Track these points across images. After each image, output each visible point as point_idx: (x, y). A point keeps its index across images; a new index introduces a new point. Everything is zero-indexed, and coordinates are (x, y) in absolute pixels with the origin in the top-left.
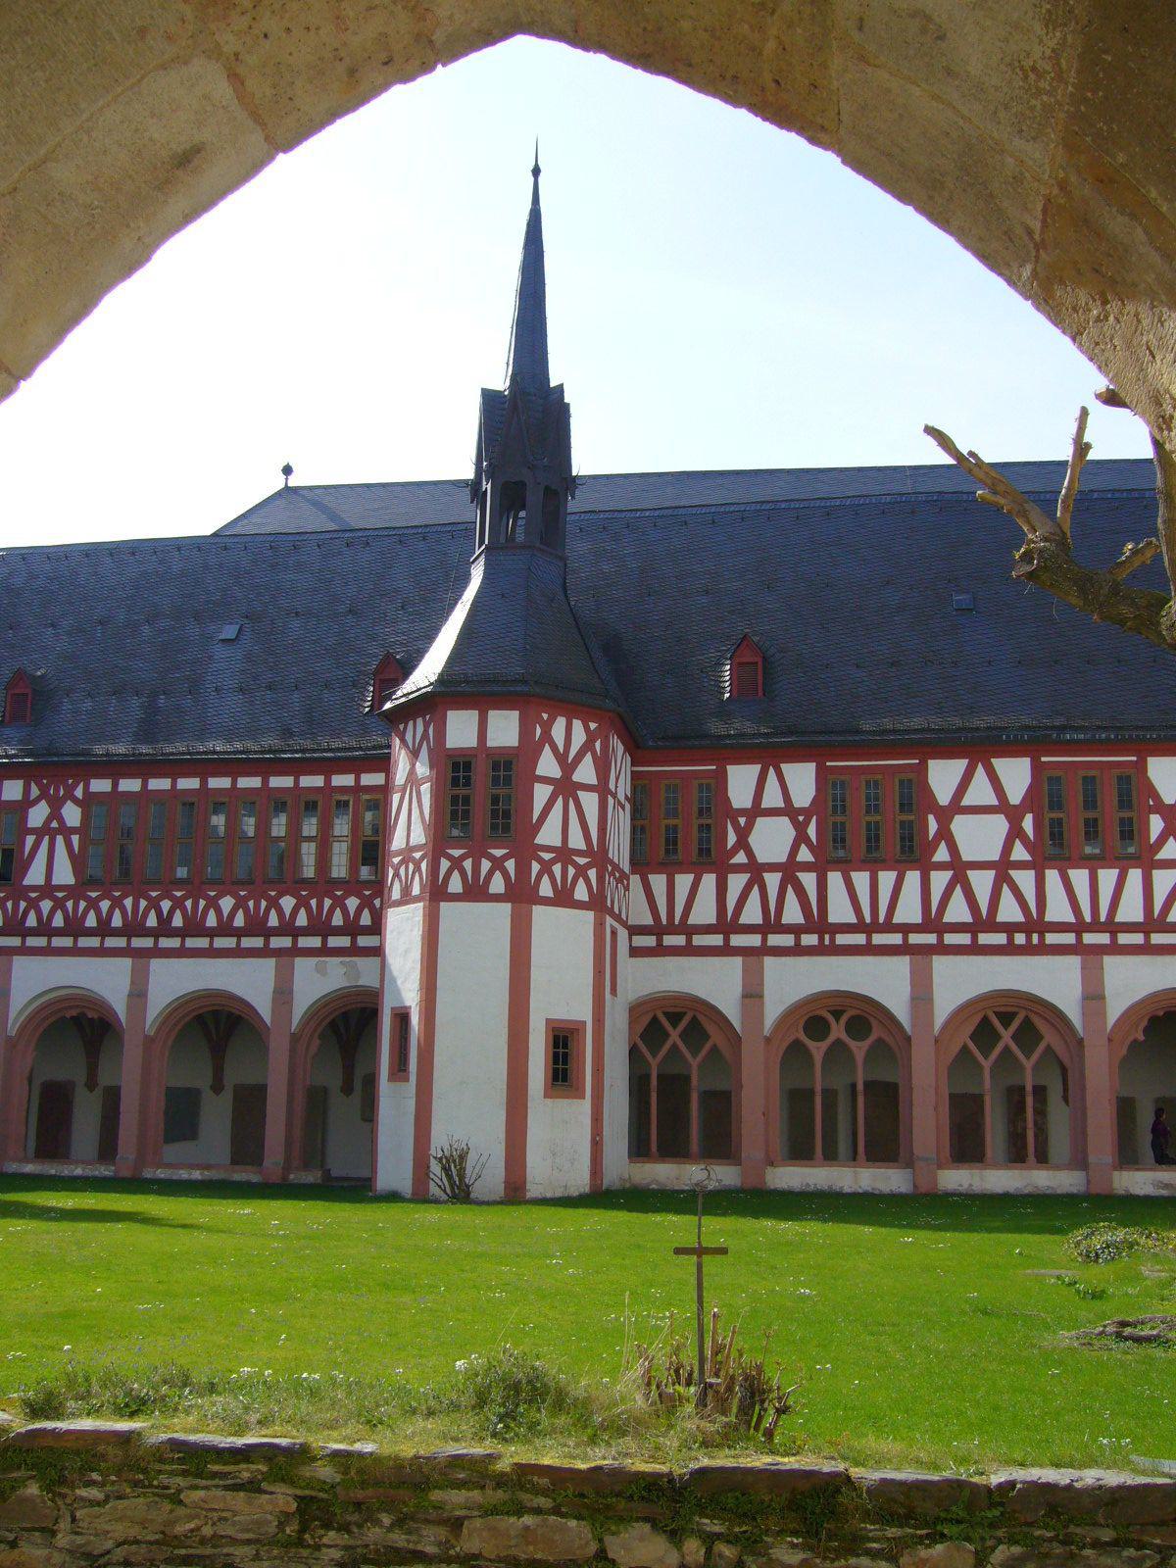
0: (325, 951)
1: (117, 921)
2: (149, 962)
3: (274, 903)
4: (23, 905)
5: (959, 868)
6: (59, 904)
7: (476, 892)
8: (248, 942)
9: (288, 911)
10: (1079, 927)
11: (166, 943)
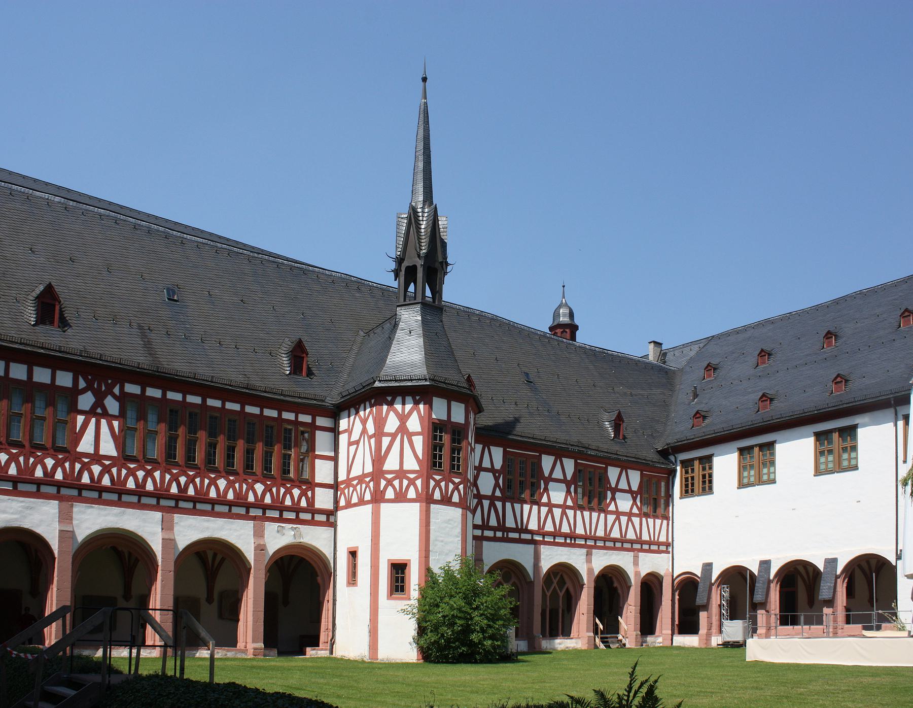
0: (281, 520)
1: (150, 486)
2: (263, 526)
3: (251, 488)
4: (78, 466)
5: (550, 506)
6: (106, 470)
7: (446, 501)
8: (235, 510)
9: (259, 493)
10: (586, 538)
11: (182, 504)
